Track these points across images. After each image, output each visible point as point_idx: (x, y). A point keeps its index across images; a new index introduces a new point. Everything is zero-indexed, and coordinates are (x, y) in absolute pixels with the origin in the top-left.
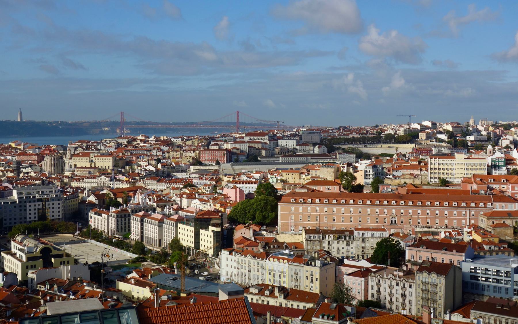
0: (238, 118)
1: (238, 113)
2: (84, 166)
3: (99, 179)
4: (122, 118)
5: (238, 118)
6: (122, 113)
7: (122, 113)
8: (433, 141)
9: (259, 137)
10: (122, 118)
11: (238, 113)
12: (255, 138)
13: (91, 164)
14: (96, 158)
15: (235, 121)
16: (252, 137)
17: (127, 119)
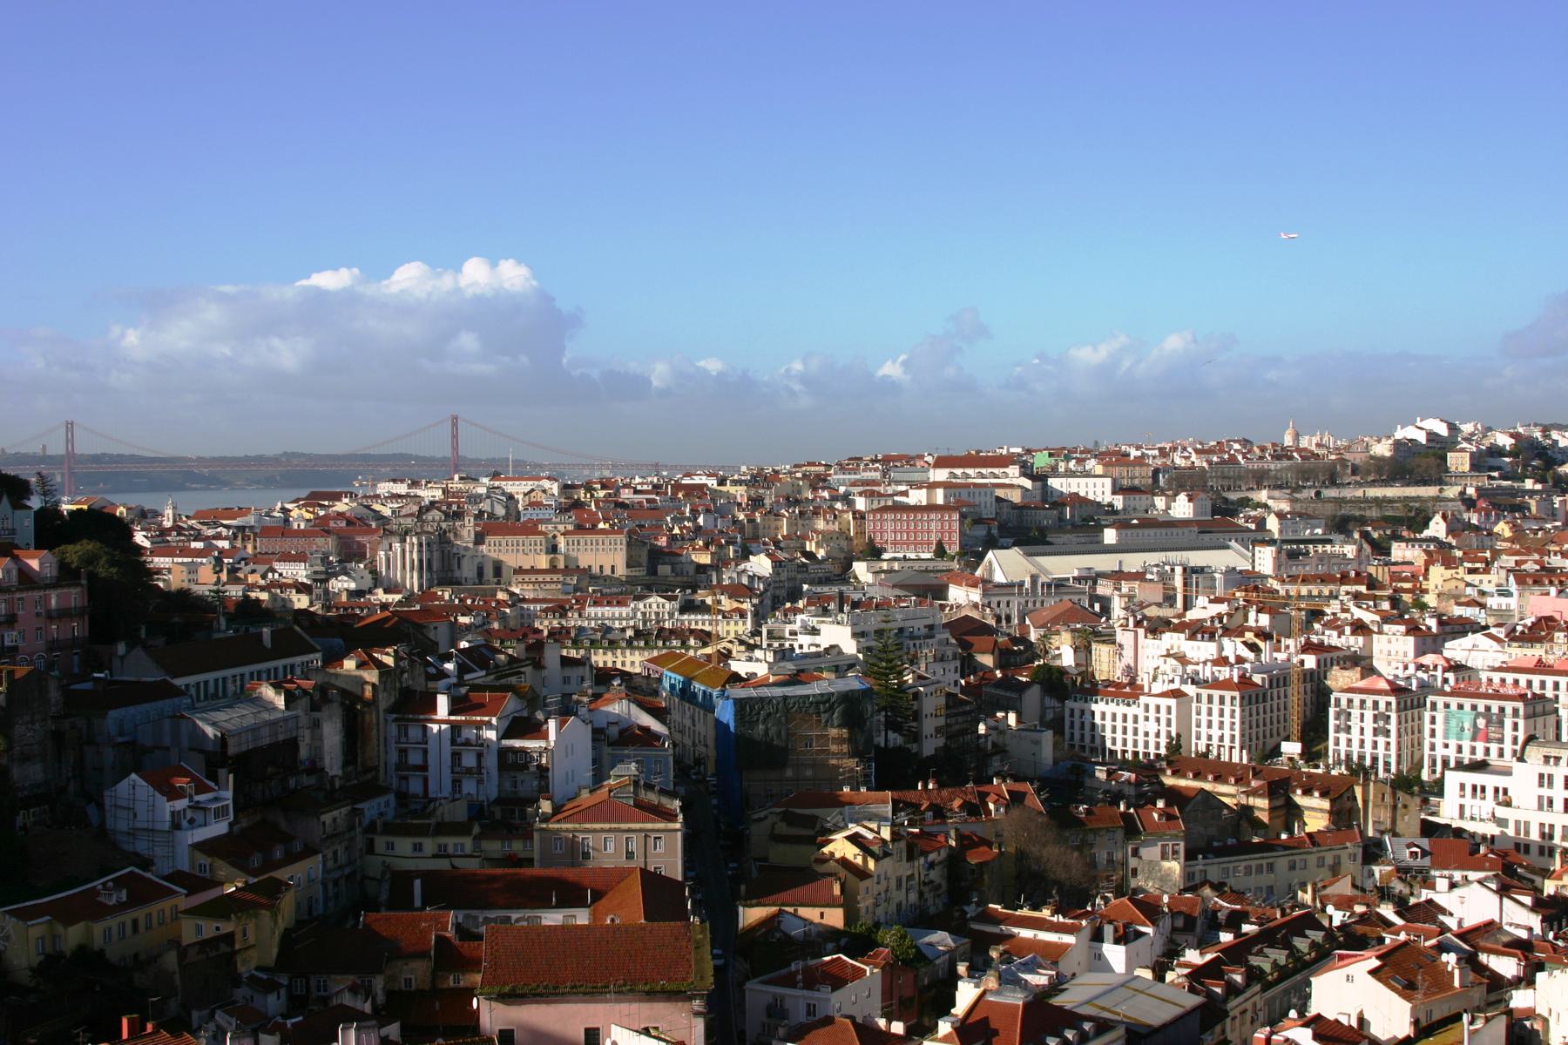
0: (455, 437)
1: (455, 421)
2: (527, 567)
3: (641, 605)
4: (70, 441)
5: (455, 437)
6: (70, 426)
7: (70, 426)
8: (1493, 478)
9: (984, 471)
10: (70, 441)
11: (455, 421)
12: (970, 471)
13: (552, 561)
14: (570, 538)
15: (448, 453)
16: (958, 471)
17: (84, 447)
